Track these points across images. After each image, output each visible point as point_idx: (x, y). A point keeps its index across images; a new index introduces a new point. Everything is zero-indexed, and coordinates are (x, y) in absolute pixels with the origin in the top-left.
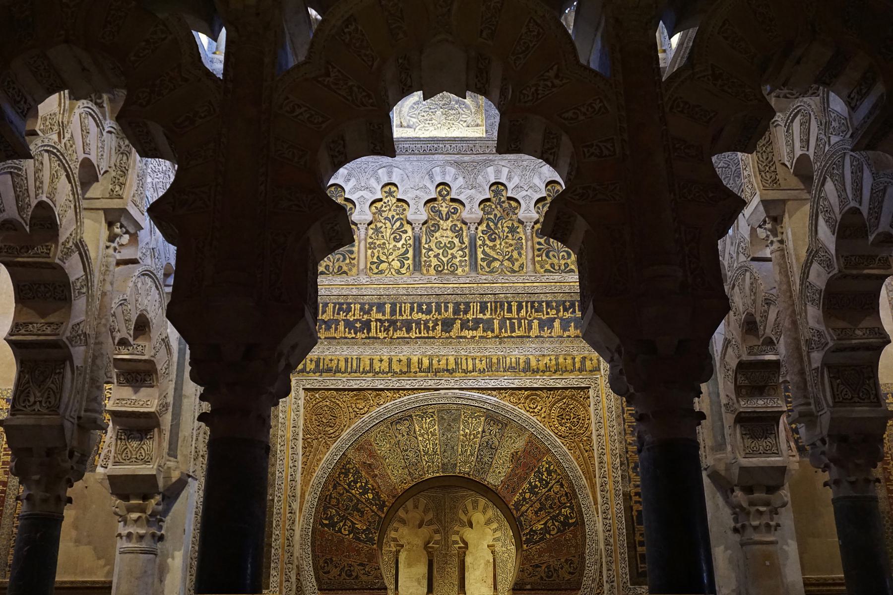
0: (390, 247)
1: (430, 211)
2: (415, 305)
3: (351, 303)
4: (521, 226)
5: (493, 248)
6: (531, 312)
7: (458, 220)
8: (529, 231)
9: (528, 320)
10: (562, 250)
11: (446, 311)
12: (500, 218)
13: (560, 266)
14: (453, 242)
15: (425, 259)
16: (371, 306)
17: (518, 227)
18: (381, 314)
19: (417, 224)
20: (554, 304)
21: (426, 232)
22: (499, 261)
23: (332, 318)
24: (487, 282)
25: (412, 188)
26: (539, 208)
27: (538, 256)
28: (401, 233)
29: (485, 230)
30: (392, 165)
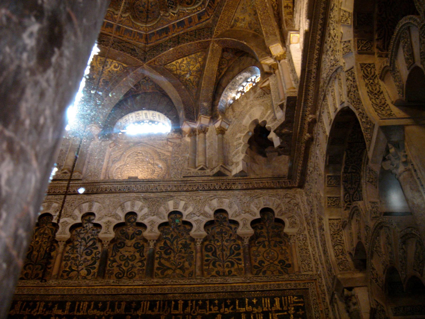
0: (82, 259)
1: (119, 233)
2: (93, 303)
3: (38, 301)
4: (193, 244)
5: (168, 260)
6: (196, 309)
7: (141, 239)
8: (199, 245)
9: (192, 315)
10: (226, 261)
11: (119, 308)
12: (177, 237)
13: (224, 273)
14: (134, 255)
15: (109, 268)
16: (54, 303)
17: (190, 244)
18: (61, 311)
19: (106, 242)
20: (216, 302)
21: (113, 248)
22: (172, 269)
23: (18, 313)
24: (158, 284)
25: (106, 216)
26: (208, 230)
27: (206, 265)
28: (93, 250)
29: (161, 247)
30: (93, 201)
